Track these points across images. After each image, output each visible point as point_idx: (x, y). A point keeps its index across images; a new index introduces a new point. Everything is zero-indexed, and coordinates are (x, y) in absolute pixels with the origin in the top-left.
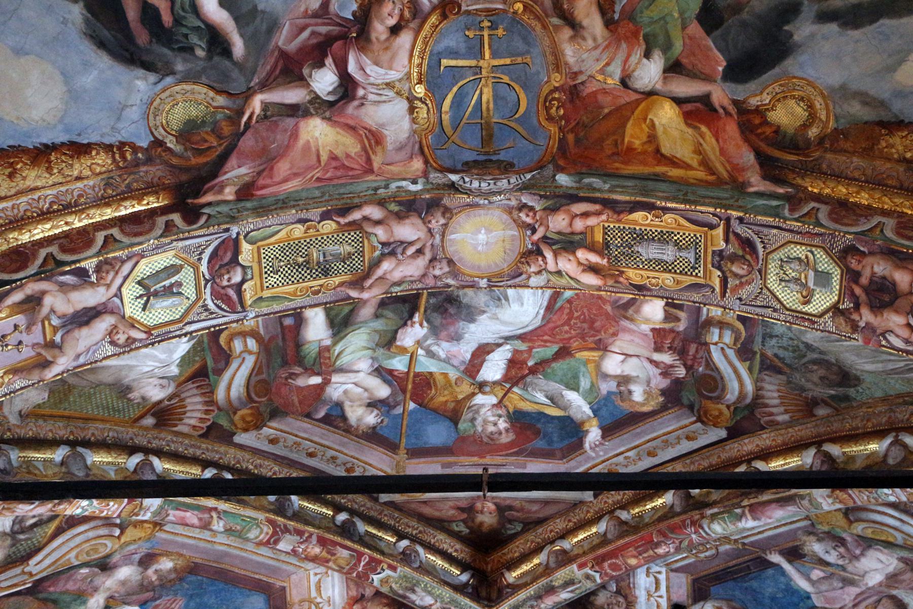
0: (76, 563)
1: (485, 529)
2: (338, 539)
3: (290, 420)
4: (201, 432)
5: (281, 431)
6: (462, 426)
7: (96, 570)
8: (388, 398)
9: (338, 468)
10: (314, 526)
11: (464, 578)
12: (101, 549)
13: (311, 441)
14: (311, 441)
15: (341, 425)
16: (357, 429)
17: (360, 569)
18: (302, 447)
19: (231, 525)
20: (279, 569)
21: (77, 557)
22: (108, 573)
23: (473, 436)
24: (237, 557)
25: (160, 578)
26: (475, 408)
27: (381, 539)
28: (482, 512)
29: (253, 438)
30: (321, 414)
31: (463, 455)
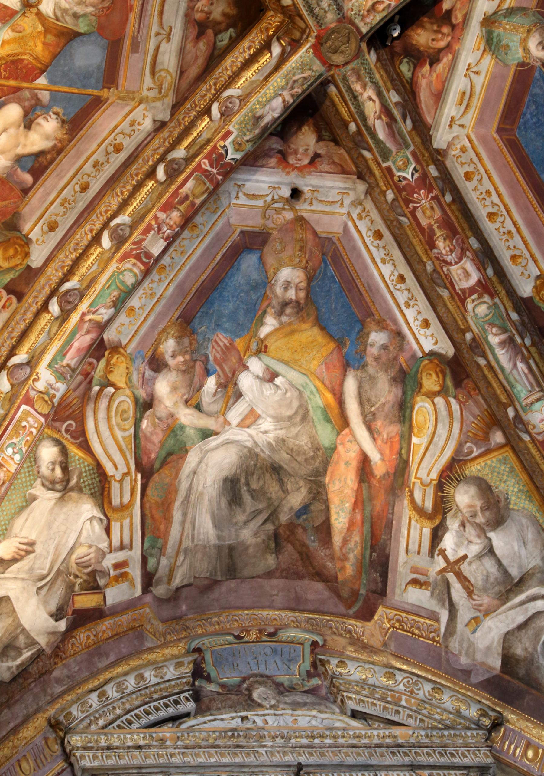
0: (132, 431)
1: (232, 11)
2: (174, 187)
3: (25, 210)
4: (14, 299)
5: (40, 219)
6: (82, 27)
7: (148, 413)
8: (24, 107)
9: (111, 160)
10: (149, 211)
11: (276, 50)
12: (125, 406)
13: (65, 187)
14: (65, 187)
15: (49, 157)
16: (60, 141)
17: (215, 171)
18: (69, 197)
19: (108, 300)
20: (217, 234)
21: (125, 430)
22: (156, 402)
23: (99, 17)
24: (187, 275)
25: (183, 353)
26: (59, 14)
27: (200, 135)
28: (210, 13)
29: (43, 246)
30: (28, 178)
31: (124, 29)
